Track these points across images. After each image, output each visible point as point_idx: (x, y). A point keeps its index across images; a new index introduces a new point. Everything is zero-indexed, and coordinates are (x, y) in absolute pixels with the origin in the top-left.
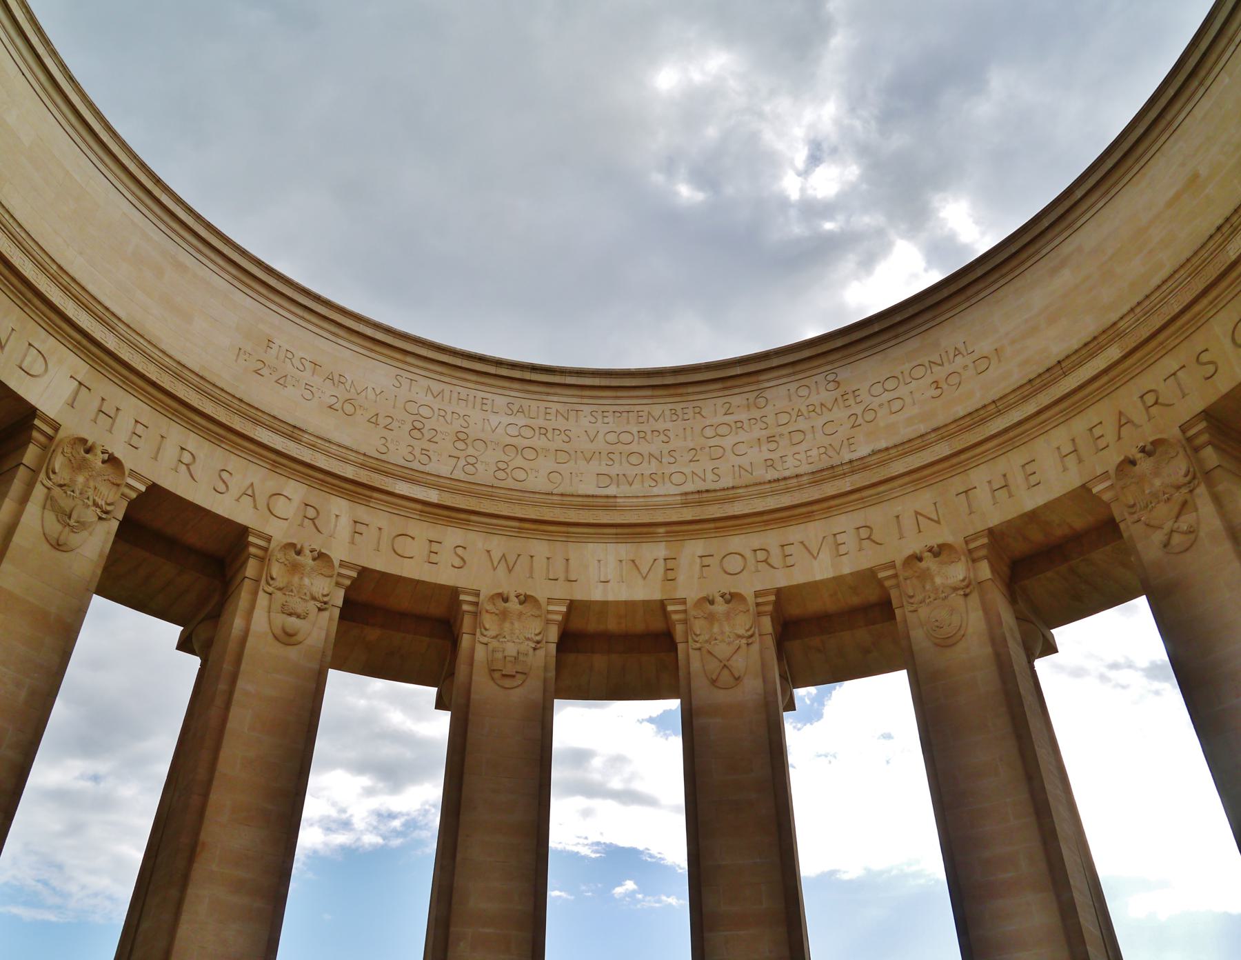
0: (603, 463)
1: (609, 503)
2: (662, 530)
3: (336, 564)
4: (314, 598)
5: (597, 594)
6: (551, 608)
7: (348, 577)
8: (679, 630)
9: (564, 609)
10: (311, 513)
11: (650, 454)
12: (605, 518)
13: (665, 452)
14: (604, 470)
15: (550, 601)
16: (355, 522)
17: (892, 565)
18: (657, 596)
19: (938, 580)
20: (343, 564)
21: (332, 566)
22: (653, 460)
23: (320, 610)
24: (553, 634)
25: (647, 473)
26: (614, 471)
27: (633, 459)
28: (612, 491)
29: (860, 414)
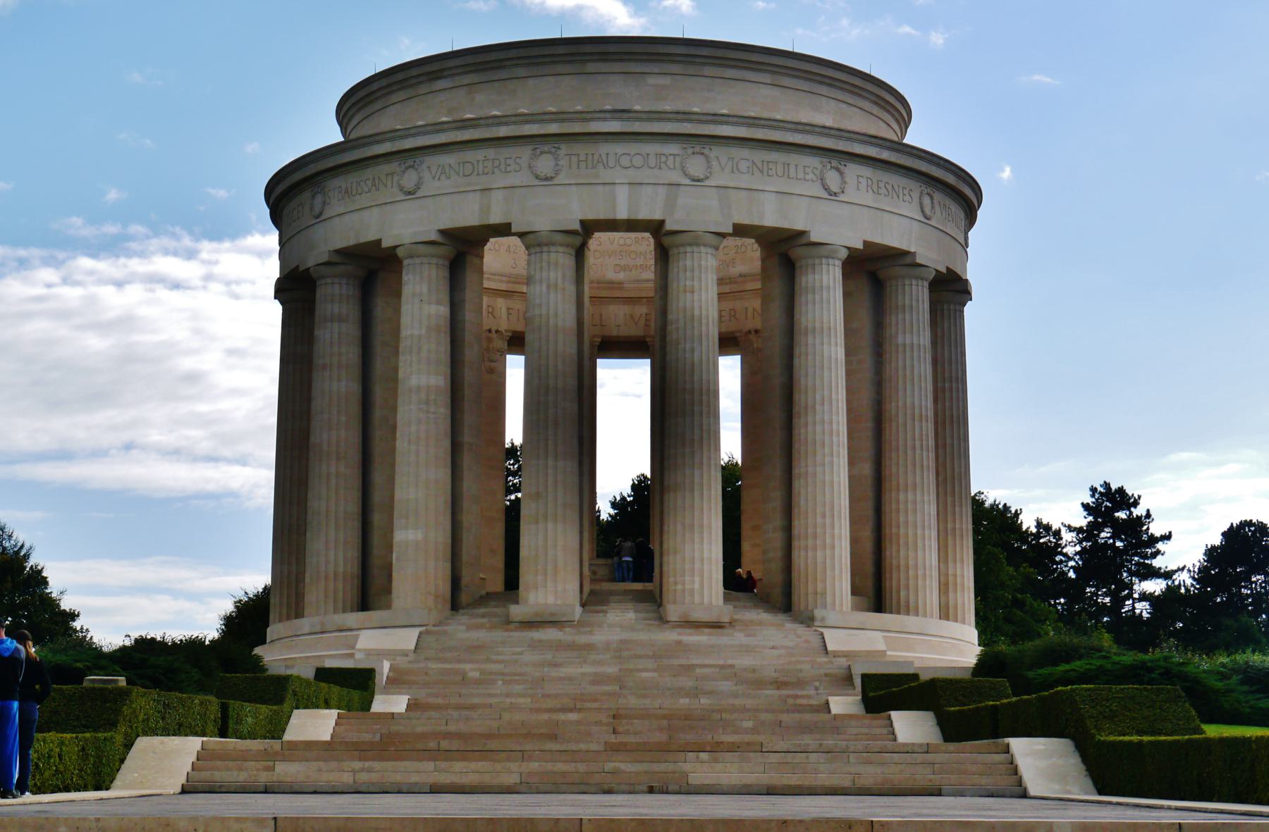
0: (618, 258)
1: (619, 285)
2: (645, 300)
3: (504, 332)
4: (498, 351)
5: (614, 333)
6: (596, 339)
7: (507, 336)
8: (651, 348)
9: (600, 340)
10: (491, 310)
11: (641, 253)
12: (617, 294)
13: (648, 252)
14: (617, 262)
15: (594, 336)
16: (508, 309)
17: (741, 331)
18: (641, 333)
19: (755, 346)
20: (506, 331)
21: (503, 334)
22: (642, 256)
23: (501, 355)
24: (596, 349)
25: (639, 264)
26: (623, 262)
27: (633, 256)
28: (621, 276)
29: (740, 245)
